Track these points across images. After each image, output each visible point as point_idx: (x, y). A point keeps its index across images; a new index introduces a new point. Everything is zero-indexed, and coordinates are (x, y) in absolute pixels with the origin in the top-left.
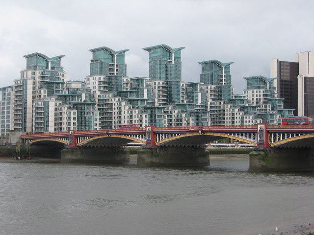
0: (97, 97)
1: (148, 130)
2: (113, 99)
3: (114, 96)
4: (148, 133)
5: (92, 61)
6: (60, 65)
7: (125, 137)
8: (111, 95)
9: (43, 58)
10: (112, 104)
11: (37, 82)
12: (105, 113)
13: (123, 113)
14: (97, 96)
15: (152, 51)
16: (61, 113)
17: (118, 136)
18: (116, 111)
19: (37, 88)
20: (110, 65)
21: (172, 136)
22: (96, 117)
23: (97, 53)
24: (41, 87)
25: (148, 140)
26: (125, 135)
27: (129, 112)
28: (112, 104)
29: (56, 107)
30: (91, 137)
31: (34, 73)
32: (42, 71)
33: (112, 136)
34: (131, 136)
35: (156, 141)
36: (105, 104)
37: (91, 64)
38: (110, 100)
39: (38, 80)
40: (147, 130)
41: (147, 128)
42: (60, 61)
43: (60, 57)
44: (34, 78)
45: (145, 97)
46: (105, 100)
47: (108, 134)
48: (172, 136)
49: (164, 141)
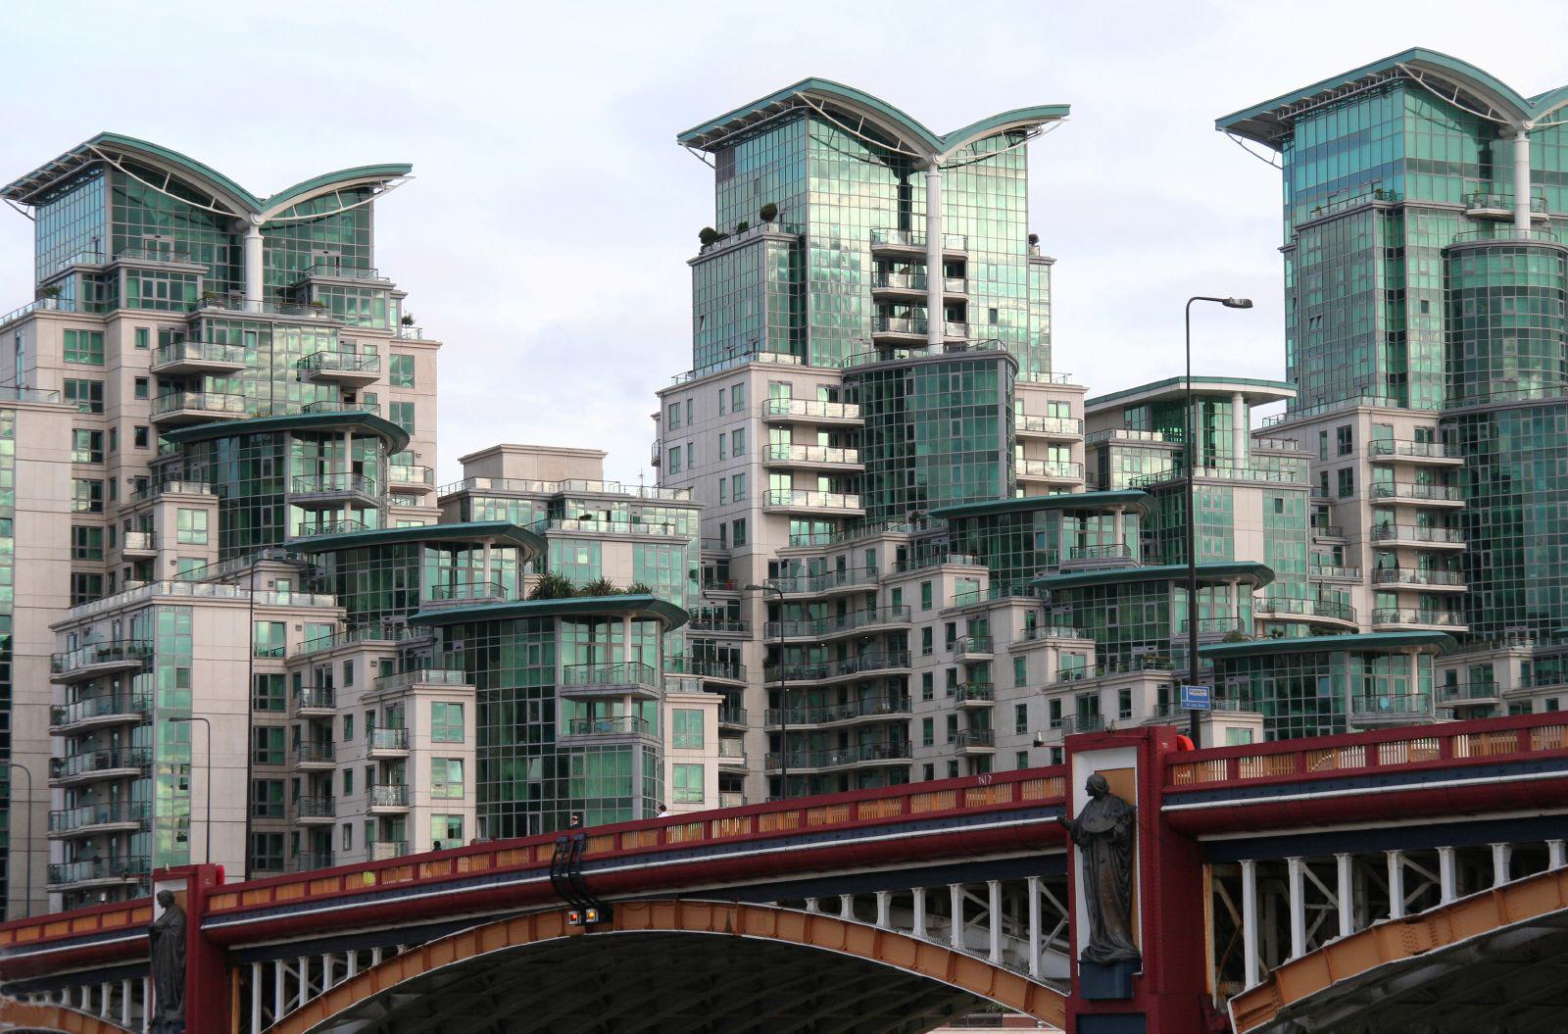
0: (759, 574)
1: (1098, 788)
2: (911, 593)
3: (916, 556)
4: (1089, 841)
5: (708, 237)
6: (365, 264)
7: (791, 933)
8: (888, 554)
9: (177, 187)
10: (897, 640)
11: (127, 437)
12: (843, 735)
13: (1003, 722)
14: (759, 574)
15: (1307, 135)
16: (322, 729)
17: (699, 922)
18: (943, 704)
19: (126, 492)
20: (885, 260)
21: (1475, 873)
22: (692, 757)
23: (750, 155)
24: (153, 484)
25: (1095, 963)
26: (792, 897)
27: (1069, 707)
28: (897, 640)
29: (274, 667)
30: (390, 957)
31: (96, 346)
32: (173, 319)
33: (635, 924)
34: (865, 908)
35: (1233, 969)
36: (840, 647)
37: (693, 263)
38: (885, 599)
39: (132, 410)
40: (1081, 799)
41: (1083, 769)
42: (362, 220)
43: (362, 186)
44: (95, 395)
45: (1248, 549)
46: (841, 604)
47: (571, 890)
48: (1475, 873)
49: (1355, 965)
